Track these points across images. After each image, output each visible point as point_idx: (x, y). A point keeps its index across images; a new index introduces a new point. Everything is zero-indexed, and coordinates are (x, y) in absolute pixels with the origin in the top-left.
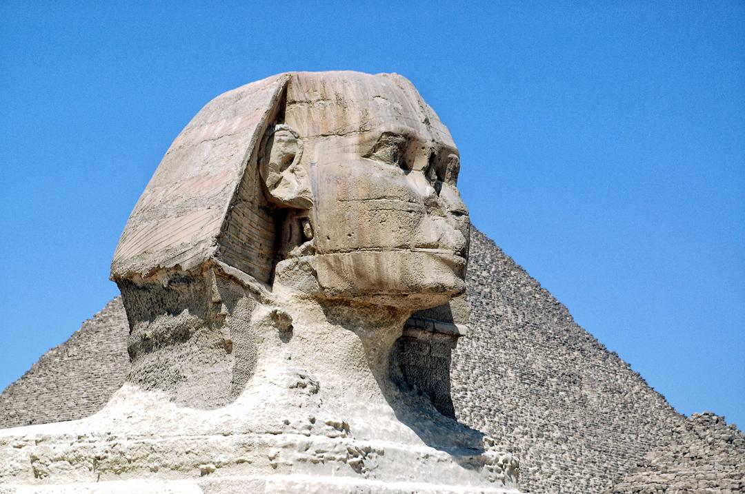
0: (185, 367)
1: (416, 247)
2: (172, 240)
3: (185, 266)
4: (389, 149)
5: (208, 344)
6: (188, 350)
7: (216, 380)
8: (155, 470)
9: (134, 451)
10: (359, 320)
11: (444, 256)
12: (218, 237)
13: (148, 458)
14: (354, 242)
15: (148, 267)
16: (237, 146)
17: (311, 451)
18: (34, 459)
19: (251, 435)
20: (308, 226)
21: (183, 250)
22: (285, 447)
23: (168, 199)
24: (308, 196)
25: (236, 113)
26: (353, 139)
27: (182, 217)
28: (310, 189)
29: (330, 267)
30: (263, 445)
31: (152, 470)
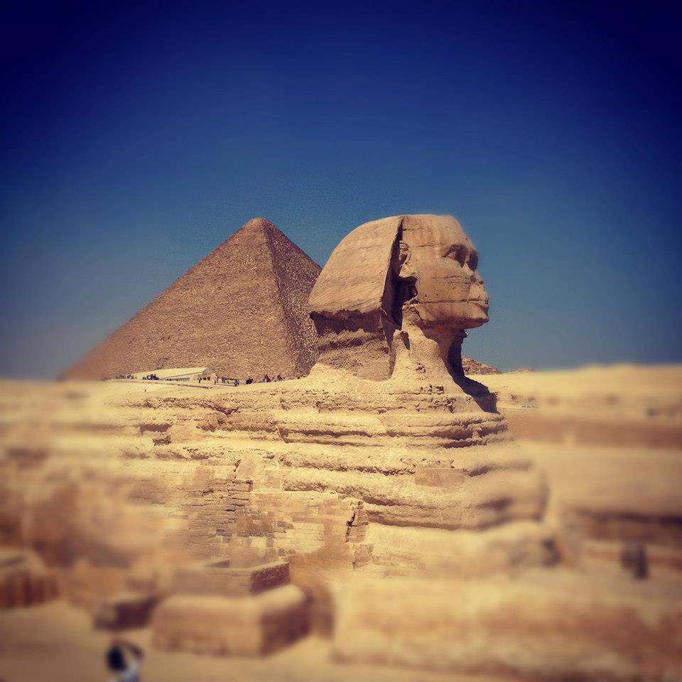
0: (360, 358)
2: (351, 297)
3: (363, 311)
4: (454, 253)
6: (361, 350)
8: (352, 409)
10: (438, 335)
12: (382, 297)
14: (440, 299)
18: (282, 401)
19: (406, 394)
25: (377, 235)
26: (437, 249)
29: (427, 310)
30: (412, 399)
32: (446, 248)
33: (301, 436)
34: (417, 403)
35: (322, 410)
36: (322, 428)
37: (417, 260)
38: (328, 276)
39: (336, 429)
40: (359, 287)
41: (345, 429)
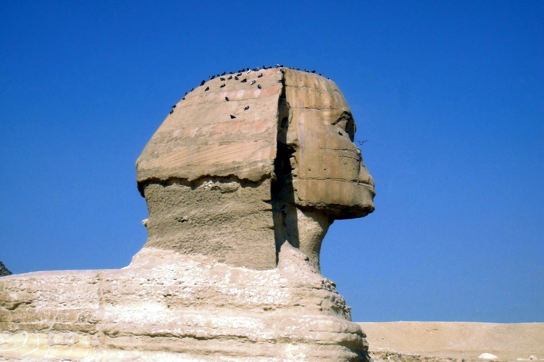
1: (360, 182)
3: (242, 177)
4: (345, 121)
5: (251, 228)
6: (230, 229)
7: (262, 251)
8: (223, 305)
9: (201, 293)
11: (371, 189)
13: (213, 298)
15: (197, 175)
16: (265, 106)
17: (335, 302)
19: (303, 288)
20: (292, 160)
21: (236, 166)
22: (325, 298)
23: (204, 133)
24: (298, 143)
26: (326, 113)
27: (226, 146)
28: (299, 139)
29: (307, 188)
31: (217, 306)
32: (338, 115)
33: (139, 342)
34: (318, 301)
35: (172, 306)
36: (178, 331)
37: (300, 124)
38: (176, 134)
39: (199, 332)
40: (233, 147)
41: (214, 333)
